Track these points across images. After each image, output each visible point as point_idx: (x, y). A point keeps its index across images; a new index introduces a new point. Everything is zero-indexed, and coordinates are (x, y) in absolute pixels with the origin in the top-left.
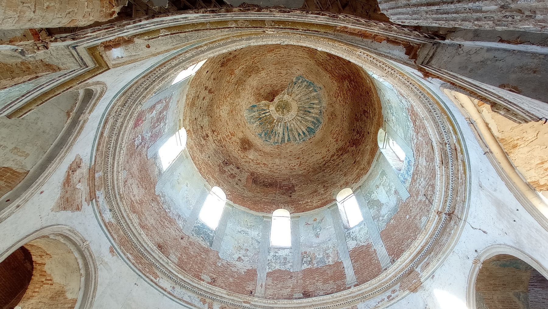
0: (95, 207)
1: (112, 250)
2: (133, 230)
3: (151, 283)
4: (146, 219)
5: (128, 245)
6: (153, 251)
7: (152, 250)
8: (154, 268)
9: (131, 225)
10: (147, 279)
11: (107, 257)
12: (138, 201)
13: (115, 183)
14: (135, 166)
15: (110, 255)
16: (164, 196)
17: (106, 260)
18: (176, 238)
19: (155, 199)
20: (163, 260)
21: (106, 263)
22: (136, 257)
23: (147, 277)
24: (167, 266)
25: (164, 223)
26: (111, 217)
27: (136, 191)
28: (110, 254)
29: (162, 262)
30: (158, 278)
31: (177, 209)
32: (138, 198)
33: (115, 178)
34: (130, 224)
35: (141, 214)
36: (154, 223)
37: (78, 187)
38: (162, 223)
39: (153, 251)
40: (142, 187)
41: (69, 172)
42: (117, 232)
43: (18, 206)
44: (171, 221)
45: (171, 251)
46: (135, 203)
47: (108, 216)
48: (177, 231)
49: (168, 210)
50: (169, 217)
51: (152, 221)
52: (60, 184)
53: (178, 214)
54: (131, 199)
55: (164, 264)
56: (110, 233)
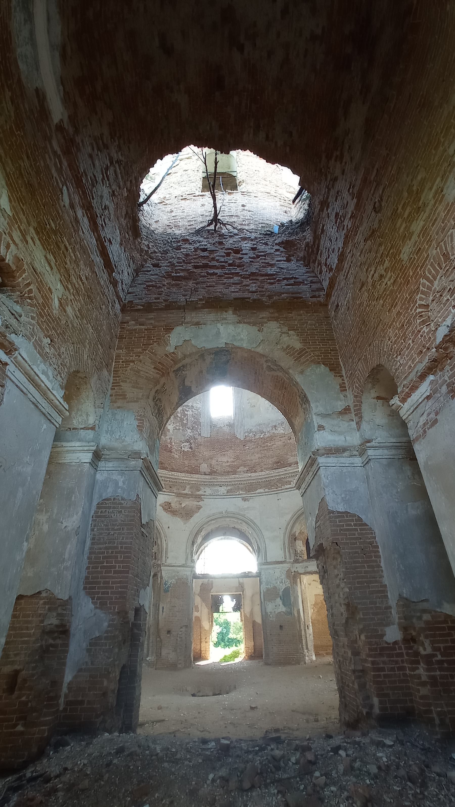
0: (208, 497)
1: (244, 499)
2: (244, 479)
3: (288, 490)
4: (251, 460)
5: (254, 486)
6: (271, 474)
7: (268, 474)
8: (284, 480)
9: (239, 479)
10: (283, 491)
11: (246, 504)
12: (234, 460)
13: (200, 480)
14: (205, 453)
15: (247, 502)
16: (251, 431)
17: (246, 507)
18: (285, 443)
19: (245, 443)
20: (282, 472)
21: (248, 508)
22: (266, 486)
23: (282, 490)
24: (288, 472)
25: (267, 446)
26: (225, 488)
27: (225, 459)
28: (246, 502)
29: (283, 473)
30: (292, 482)
31: (269, 424)
32: (232, 460)
33: (196, 479)
34: (237, 480)
35: (245, 462)
36: (260, 456)
37: (183, 506)
38: (266, 448)
39: (271, 474)
40: (227, 451)
41: (169, 511)
42: (239, 489)
43: (165, 540)
44: (272, 438)
45: (288, 456)
46: (233, 464)
47: (223, 490)
48: (282, 439)
49: (263, 434)
50: (268, 437)
51: (257, 456)
52: (172, 517)
53: (272, 427)
54: (227, 466)
55: (285, 473)
56: (233, 495)
